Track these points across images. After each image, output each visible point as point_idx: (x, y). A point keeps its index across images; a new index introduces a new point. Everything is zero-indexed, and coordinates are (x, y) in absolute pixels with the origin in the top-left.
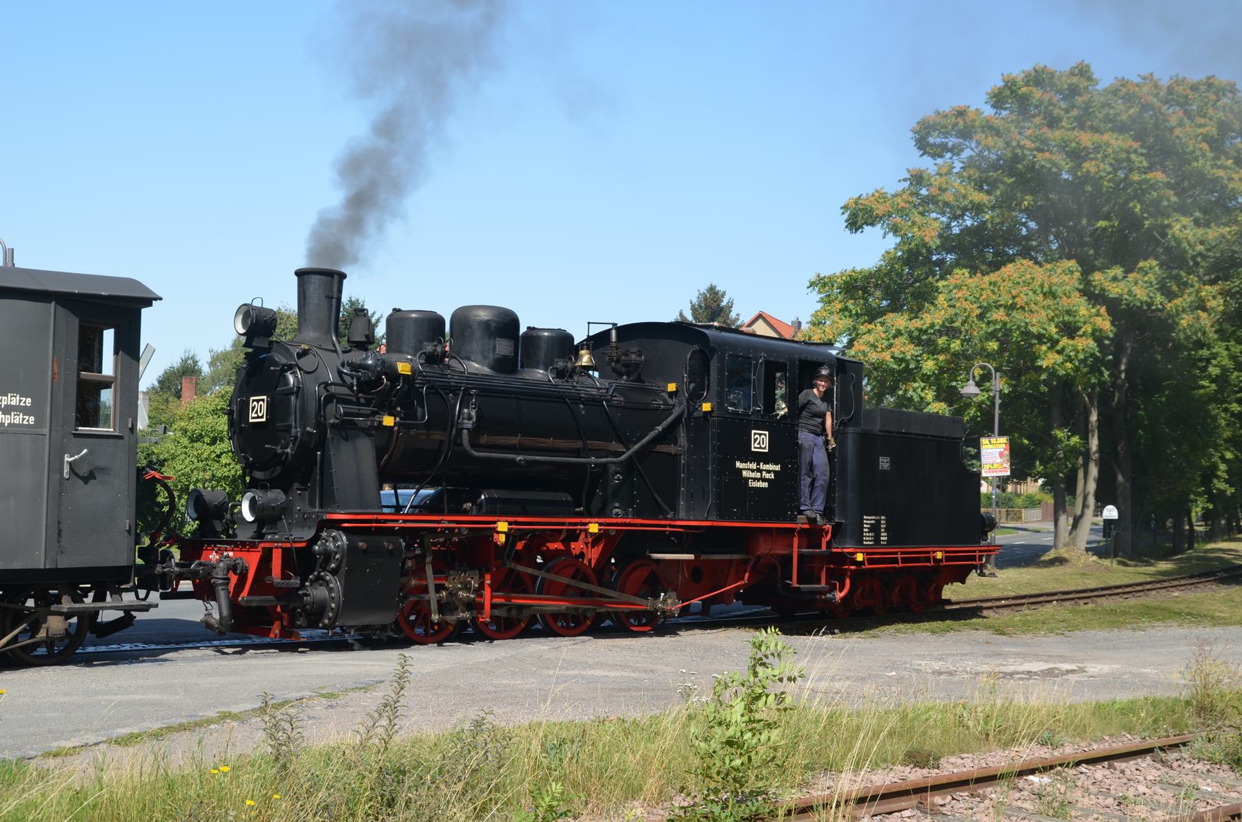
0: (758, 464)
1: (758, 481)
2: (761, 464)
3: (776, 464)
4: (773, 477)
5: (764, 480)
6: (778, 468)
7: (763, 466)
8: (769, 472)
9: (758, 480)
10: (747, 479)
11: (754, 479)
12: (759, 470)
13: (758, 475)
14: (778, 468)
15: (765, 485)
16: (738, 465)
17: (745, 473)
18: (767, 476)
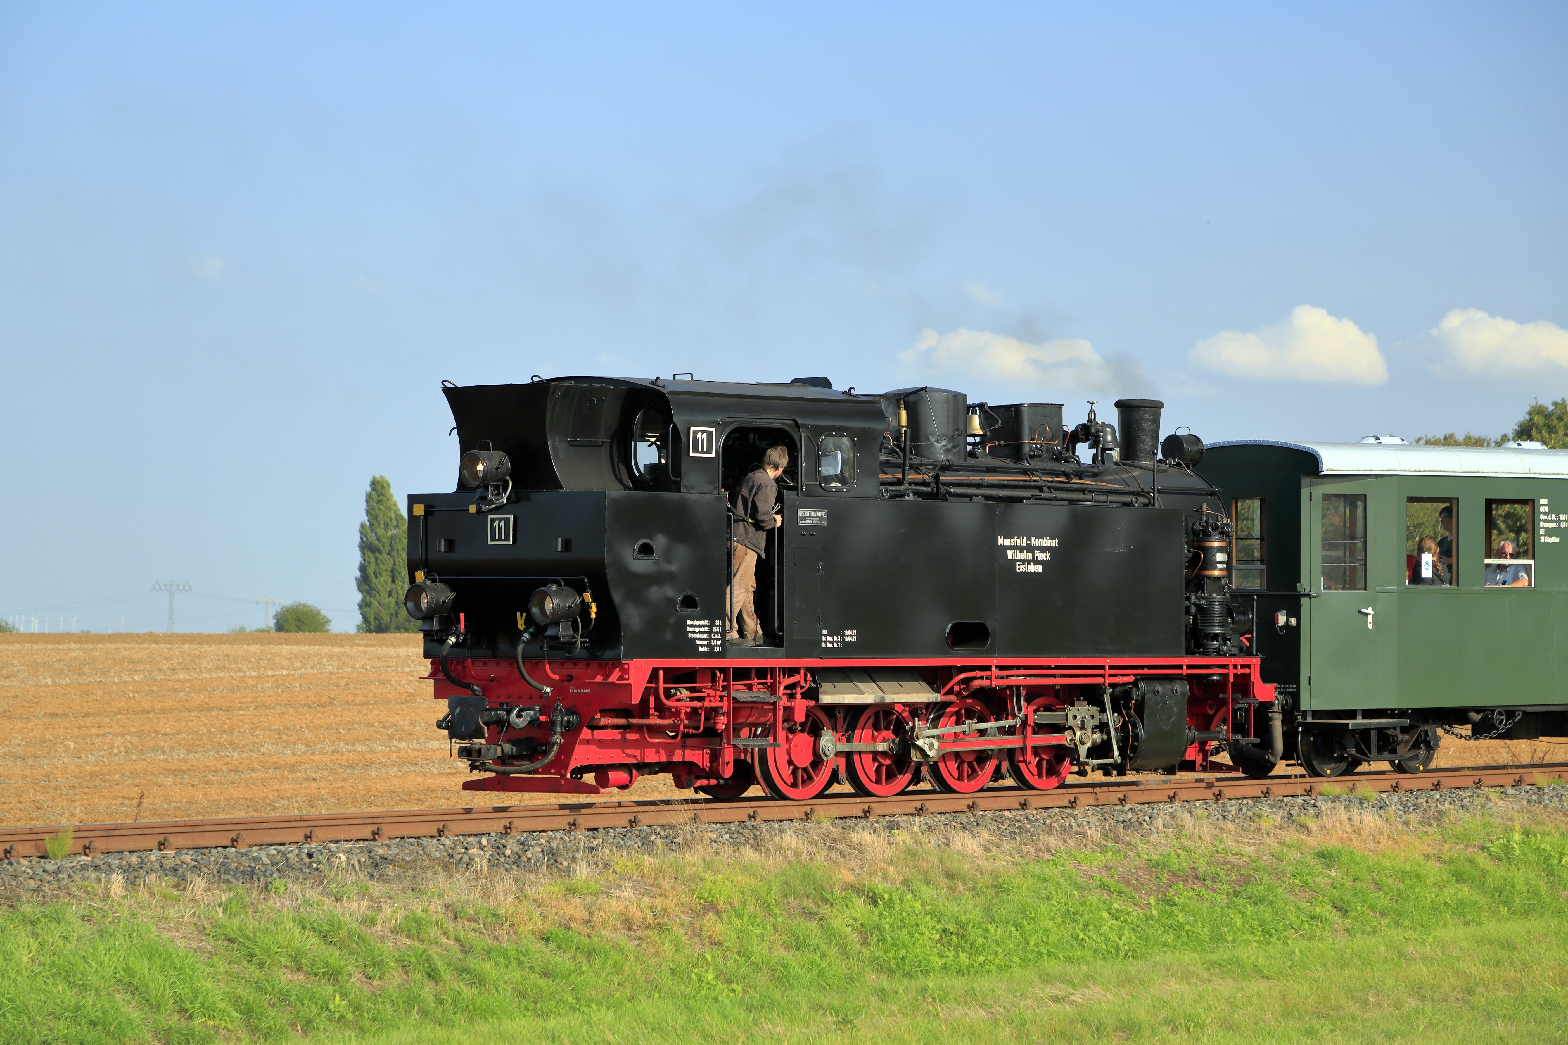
0: (1029, 539)
1: (1029, 563)
2: (1033, 539)
3: (1052, 538)
4: (1048, 558)
5: (1036, 562)
6: (1054, 543)
7: (1036, 542)
8: (1042, 549)
9: (1029, 562)
10: (1014, 562)
11: (1023, 561)
12: (1030, 549)
13: (1029, 556)
14: (1054, 543)
15: (1038, 568)
16: (1001, 541)
17: (1010, 554)
18: (1041, 556)
